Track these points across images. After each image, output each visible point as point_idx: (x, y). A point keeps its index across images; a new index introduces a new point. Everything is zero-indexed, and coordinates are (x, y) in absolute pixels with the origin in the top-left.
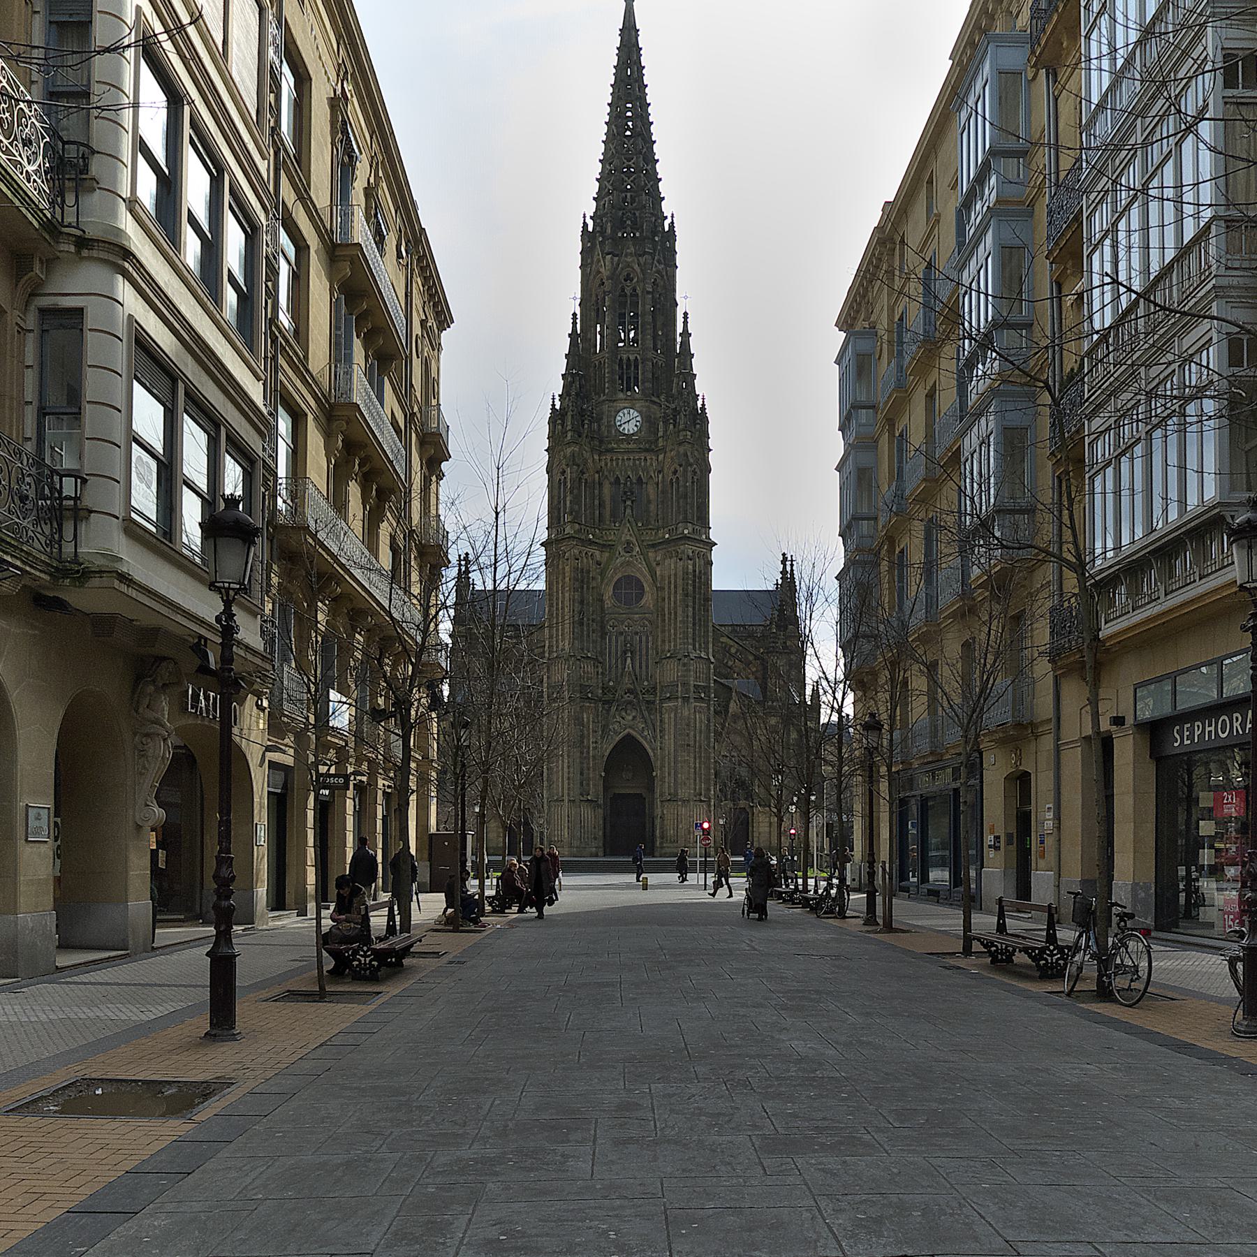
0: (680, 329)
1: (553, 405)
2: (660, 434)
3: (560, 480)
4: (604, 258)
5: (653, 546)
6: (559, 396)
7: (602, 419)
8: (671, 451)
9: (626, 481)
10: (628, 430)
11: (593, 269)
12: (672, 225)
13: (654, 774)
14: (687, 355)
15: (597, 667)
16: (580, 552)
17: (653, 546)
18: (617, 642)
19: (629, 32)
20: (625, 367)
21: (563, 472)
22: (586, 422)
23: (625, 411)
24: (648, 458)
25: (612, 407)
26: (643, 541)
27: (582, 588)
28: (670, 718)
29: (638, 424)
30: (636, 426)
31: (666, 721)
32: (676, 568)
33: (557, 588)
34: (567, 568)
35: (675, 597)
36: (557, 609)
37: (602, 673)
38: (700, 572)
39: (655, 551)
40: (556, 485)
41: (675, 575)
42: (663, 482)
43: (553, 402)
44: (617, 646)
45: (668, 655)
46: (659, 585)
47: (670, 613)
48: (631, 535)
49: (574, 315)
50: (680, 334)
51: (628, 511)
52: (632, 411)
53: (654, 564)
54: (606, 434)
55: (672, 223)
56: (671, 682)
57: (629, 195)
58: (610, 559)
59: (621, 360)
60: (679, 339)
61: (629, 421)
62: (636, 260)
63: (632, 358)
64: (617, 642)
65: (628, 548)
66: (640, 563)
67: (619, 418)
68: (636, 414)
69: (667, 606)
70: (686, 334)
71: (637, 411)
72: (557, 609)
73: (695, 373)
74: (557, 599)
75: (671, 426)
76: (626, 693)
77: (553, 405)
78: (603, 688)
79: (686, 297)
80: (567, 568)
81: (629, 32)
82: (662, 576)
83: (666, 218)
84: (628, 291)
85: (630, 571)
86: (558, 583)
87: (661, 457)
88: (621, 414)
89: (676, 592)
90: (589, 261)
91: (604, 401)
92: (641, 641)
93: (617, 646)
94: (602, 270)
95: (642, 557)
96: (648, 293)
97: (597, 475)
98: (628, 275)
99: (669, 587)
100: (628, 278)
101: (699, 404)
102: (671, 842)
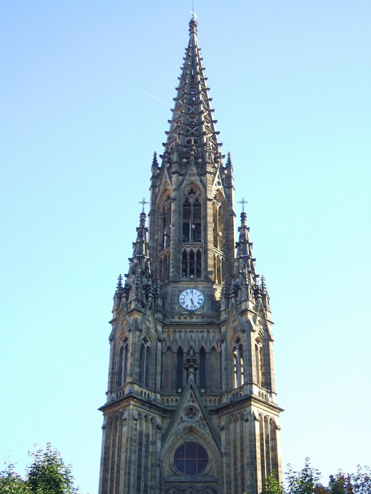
1: (120, 284)
2: (223, 308)
3: (122, 347)
4: (170, 178)
5: (217, 411)
6: (126, 275)
7: (166, 298)
8: (234, 322)
9: (189, 351)
11: (161, 188)
16: (139, 414)
17: (217, 411)
20: (188, 257)
21: (126, 339)
22: (151, 295)
23: (189, 291)
24: (211, 331)
25: (176, 287)
26: (206, 407)
27: (140, 450)
29: (201, 302)
32: (242, 431)
33: (114, 452)
35: (242, 461)
36: (112, 474)
38: (267, 436)
40: (118, 352)
42: (226, 349)
43: (120, 282)
46: (223, 450)
47: (236, 480)
48: (193, 401)
49: (143, 214)
50: (240, 229)
51: (192, 376)
52: (195, 291)
53: (218, 430)
55: (229, 159)
58: (171, 425)
59: (185, 253)
62: (198, 178)
63: (195, 250)
65: (191, 411)
66: (203, 429)
67: (183, 297)
68: (199, 293)
69: (232, 473)
70: (243, 228)
71: (200, 291)
72: (112, 474)
74: (113, 463)
75: (233, 299)
79: (243, 202)
82: (228, 443)
83: (224, 156)
84: (192, 201)
85: (191, 438)
86: (114, 446)
87: (223, 329)
88: (184, 293)
89: (242, 456)
94: (168, 187)
95: (205, 422)
97: (159, 344)
99: (235, 452)
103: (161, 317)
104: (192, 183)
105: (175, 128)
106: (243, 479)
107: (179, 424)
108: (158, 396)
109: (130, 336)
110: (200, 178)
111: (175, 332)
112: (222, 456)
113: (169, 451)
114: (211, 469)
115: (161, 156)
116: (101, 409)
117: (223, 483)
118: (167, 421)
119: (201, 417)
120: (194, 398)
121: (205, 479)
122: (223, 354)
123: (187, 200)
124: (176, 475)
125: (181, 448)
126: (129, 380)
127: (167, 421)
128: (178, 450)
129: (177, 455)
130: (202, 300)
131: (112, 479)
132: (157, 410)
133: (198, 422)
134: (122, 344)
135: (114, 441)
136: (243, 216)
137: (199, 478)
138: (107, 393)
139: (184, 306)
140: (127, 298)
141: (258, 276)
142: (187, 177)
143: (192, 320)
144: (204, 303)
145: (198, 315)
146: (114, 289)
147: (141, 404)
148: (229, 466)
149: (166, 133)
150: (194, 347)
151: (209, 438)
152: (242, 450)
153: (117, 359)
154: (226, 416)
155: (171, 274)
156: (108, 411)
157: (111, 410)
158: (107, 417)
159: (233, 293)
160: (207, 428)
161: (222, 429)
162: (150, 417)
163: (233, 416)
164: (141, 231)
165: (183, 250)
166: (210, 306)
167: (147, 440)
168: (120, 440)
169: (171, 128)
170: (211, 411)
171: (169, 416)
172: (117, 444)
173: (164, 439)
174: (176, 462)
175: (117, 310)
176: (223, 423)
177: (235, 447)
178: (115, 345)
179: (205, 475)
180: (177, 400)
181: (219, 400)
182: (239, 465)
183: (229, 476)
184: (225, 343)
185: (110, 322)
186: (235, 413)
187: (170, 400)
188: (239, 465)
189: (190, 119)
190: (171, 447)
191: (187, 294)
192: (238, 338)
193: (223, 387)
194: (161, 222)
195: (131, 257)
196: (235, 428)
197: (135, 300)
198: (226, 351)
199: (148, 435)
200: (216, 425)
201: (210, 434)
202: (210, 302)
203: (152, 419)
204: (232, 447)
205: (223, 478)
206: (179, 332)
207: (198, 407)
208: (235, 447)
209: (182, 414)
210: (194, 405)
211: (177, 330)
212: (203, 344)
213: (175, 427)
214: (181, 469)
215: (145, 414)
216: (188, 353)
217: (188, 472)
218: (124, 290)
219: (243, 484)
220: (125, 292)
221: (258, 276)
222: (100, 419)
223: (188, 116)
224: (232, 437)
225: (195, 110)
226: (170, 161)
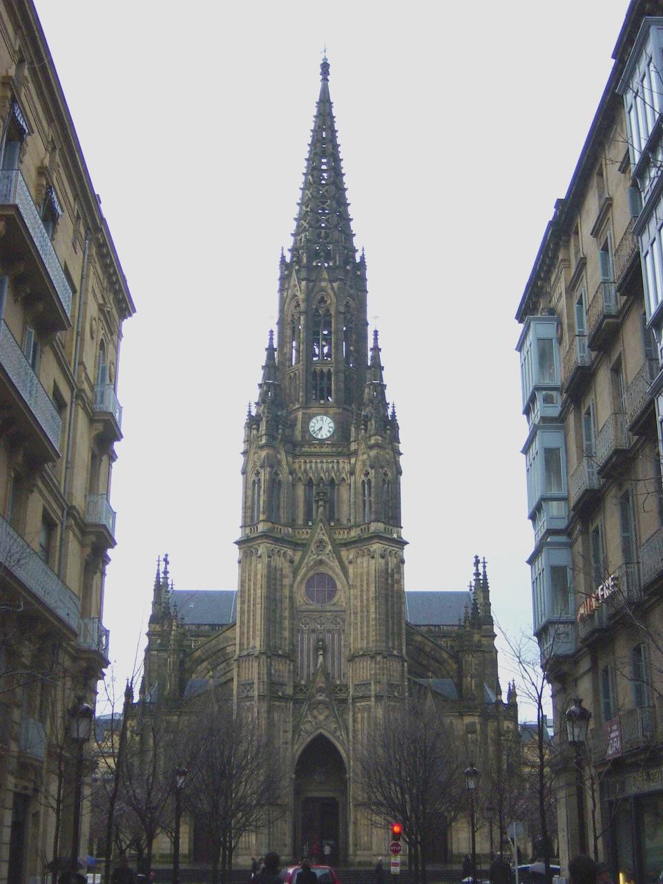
0: (370, 344)
1: (250, 412)
3: (254, 481)
4: (299, 283)
10: (322, 435)
12: (363, 258)
13: (347, 776)
14: (378, 367)
18: (309, 639)
19: (325, 103)
21: (258, 473)
23: (319, 418)
24: (340, 461)
28: (363, 718)
30: (329, 431)
31: (359, 720)
32: (368, 566)
33: (249, 586)
34: (259, 566)
35: (368, 595)
36: (249, 606)
37: (294, 671)
39: (348, 550)
40: (250, 486)
41: (368, 573)
43: (250, 409)
44: (309, 643)
45: (361, 653)
46: (351, 583)
48: (323, 534)
49: (271, 332)
50: (371, 349)
51: (321, 509)
52: (325, 418)
53: (346, 562)
54: (300, 439)
56: (362, 681)
57: (323, 231)
59: (315, 372)
60: (370, 354)
61: (323, 427)
63: (325, 370)
64: (309, 639)
67: (313, 424)
68: (329, 420)
69: (359, 604)
70: (376, 349)
72: (249, 606)
73: (385, 383)
74: (249, 596)
75: (363, 431)
76: (318, 692)
77: (250, 412)
78: (295, 687)
79: (376, 317)
80: (259, 566)
81: (325, 103)
82: (356, 576)
85: (322, 569)
86: (249, 580)
87: (353, 461)
88: (314, 420)
89: (368, 590)
90: (286, 286)
91: (298, 408)
92: (333, 640)
93: (309, 643)
94: (298, 293)
95: (334, 555)
96: (341, 313)
97: (290, 477)
98: (323, 298)
99: (362, 585)
100: (322, 300)
101: (390, 412)
102: (364, 850)
104: (323, 290)
105: (305, 214)
106: (368, 611)
107: (310, 556)
108: (290, 530)
109: (262, 471)
110: (331, 285)
111: (305, 462)
112: (350, 588)
113: (301, 582)
114: (339, 599)
115: (289, 250)
116: (236, 543)
117: (350, 614)
118: (299, 554)
119: (330, 551)
120: (324, 531)
121: (333, 608)
122: (352, 487)
123: (317, 311)
124: (307, 604)
125: (312, 578)
126: (262, 517)
127: (299, 554)
128: (309, 581)
130: (331, 427)
131: (249, 611)
132: (289, 544)
133: (328, 554)
134: (253, 478)
135: (249, 575)
136: (376, 333)
137: (328, 608)
138: (241, 527)
139: (314, 435)
140: (258, 430)
141: (388, 404)
143: (322, 450)
145: (327, 444)
146: (244, 419)
148: (356, 598)
149: (295, 219)
150: (324, 478)
151: (338, 570)
152: (368, 585)
153: (250, 492)
154: (353, 550)
156: (243, 546)
157: (246, 545)
158: (242, 550)
159: (363, 424)
160: (337, 561)
161: (350, 562)
162: (282, 551)
163: (360, 550)
164: (270, 350)
166: (340, 434)
167: (281, 575)
168: (256, 575)
169: (300, 213)
170: (340, 544)
171: (301, 549)
172: (252, 578)
173: (295, 573)
174: (307, 591)
175: (248, 441)
176: (351, 557)
177: (362, 581)
178: (247, 477)
179: (334, 604)
180: (307, 532)
181: (348, 533)
182: (365, 597)
183: (356, 607)
184: (354, 477)
185: (243, 453)
186: (362, 548)
187: (301, 532)
188: (365, 597)
189: (319, 204)
190: (302, 579)
191: (317, 421)
192: (366, 471)
193: (352, 520)
194: (289, 332)
195: (260, 382)
196: (362, 563)
197: (265, 435)
198: (355, 485)
199: (282, 569)
200: (344, 559)
201: (339, 567)
204: (359, 580)
205: (350, 610)
206: (309, 462)
207: (328, 540)
208: (362, 581)
209: (313, 547)
210: (324, 538)
211: (307, 461)
213: (306, 560)
215: (277, 550)
216: (318, 485)
217: (318, 602)
218: (255, 422)
219: (368, 616)
220: (256, 424)
221: (388, 404)
222: (235, 553)
223: (318, 201)
224: (359, 571)
225: (326, 191)
226: (299, 262)
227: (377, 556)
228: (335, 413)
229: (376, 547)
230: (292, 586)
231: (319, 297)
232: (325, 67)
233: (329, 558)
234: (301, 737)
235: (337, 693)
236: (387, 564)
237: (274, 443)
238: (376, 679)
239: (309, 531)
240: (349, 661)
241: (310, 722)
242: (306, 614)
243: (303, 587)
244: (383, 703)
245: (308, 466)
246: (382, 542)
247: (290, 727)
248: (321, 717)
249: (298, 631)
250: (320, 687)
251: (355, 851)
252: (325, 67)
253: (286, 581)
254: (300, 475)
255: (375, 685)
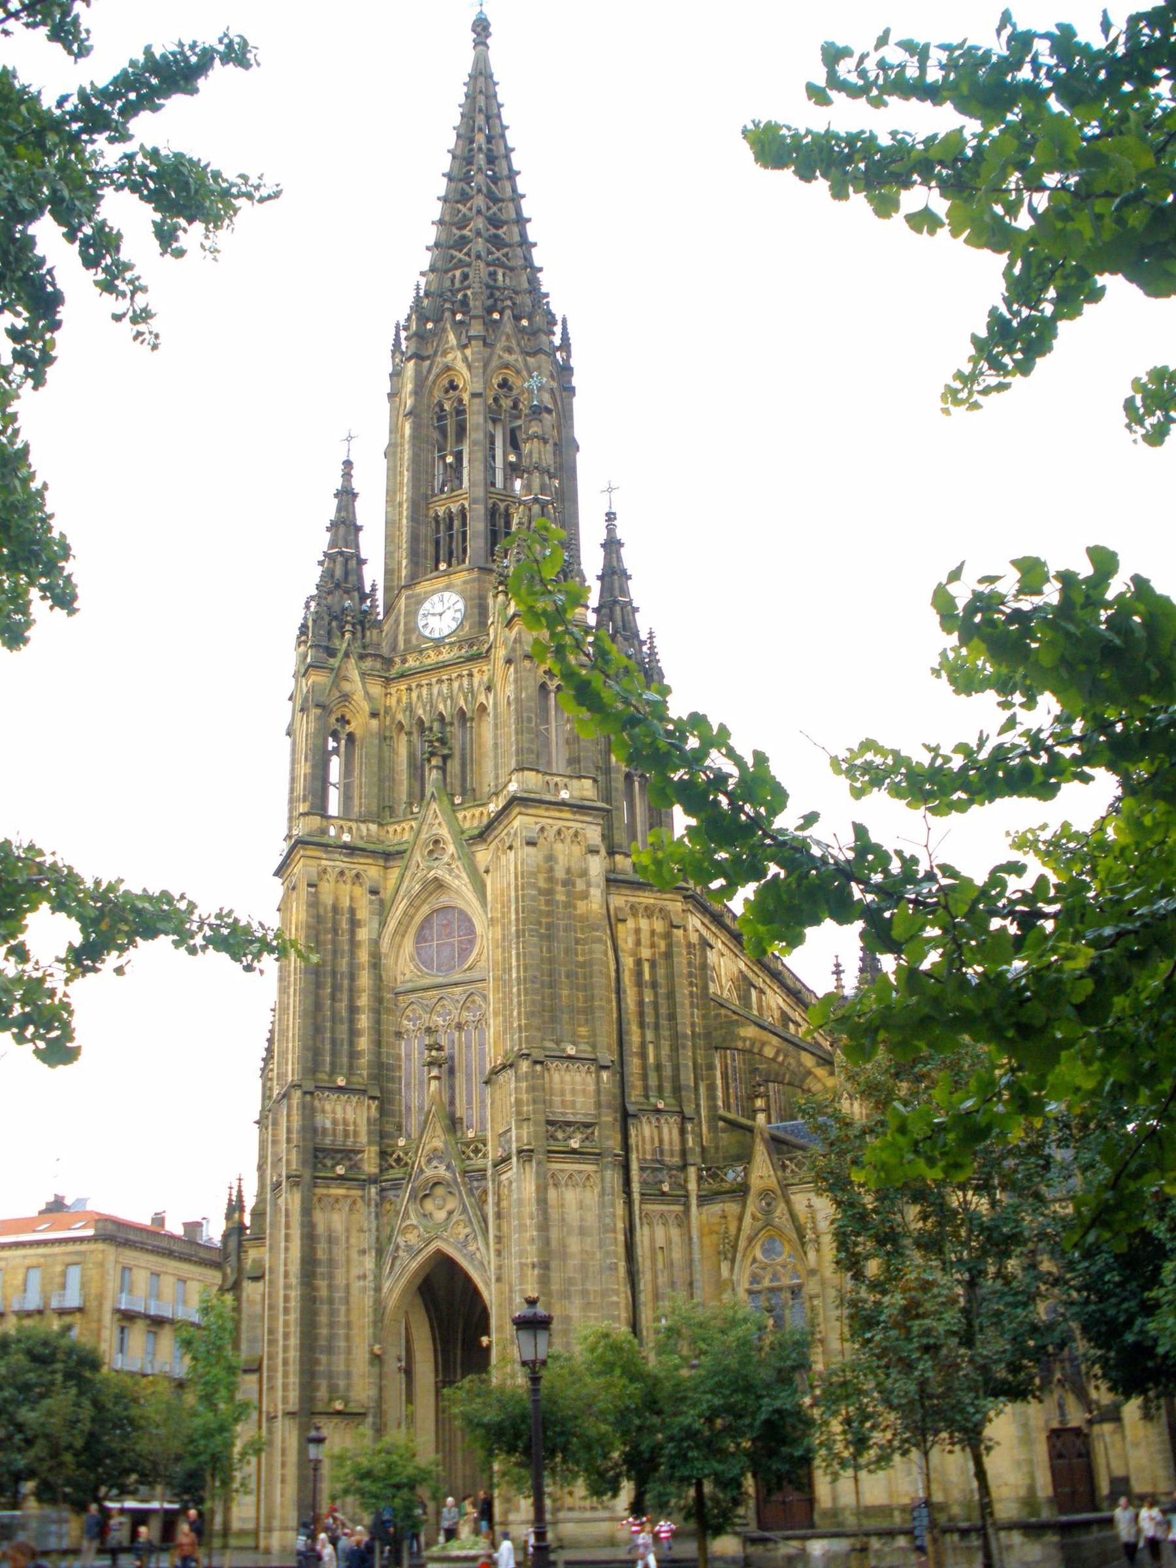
15: (369, 1107)
23: (435, 598)
24: (475, 671)
38: (568, 871)
52: (446, 594)
68: (455, 597)
78: (383, 1154)
85: (444, 900)
97: (374, 723)
103: (378, 665)
104: (448, 368)
111: (410, 689)
113: (401, 931)
120: (440, 819)
125: (427, 920)
129: (420, 937)
137: (457, 977)
139: (427, 633)
142: (439, 359)
143: (441, 658)
144: (464, 618)
145: (451, 644)
147: (327, 852)
155: (404, 573)
165: (432, 513)
170: (471, 838)
179: (469, 969)
187: (399, 829)
202: (476, 611)
203: (358, 876)
209: (417, 857)
211: (414, 685)
212: (462, 703)
214: (428, 964)
227: (517, 843)
228: (465, 582)
229: (521, 823)
230: (376, 943)
231: (446, 383)
232: (481, 28)
233: (451, 871)
234: (398, 1262)
235: (469, 1158)
236: (550, 858)
237: (333, 662)
238: (518, 1113)
239: (413, 823)
240: (486, 1083)
241: (415, 1227)
242: (413, 997)
243: (408, 945)
244: (534, 1164)
245: (414, 695)
246: (531, 811)
247: (367, 1240)
248: (441, 1215)
249: (399, 1034)
250: (435, 1150)
251: (506, 1513)
252: (481, 28)
253: (363, 934)
254: (400, 717)
255: (519, 1127)
